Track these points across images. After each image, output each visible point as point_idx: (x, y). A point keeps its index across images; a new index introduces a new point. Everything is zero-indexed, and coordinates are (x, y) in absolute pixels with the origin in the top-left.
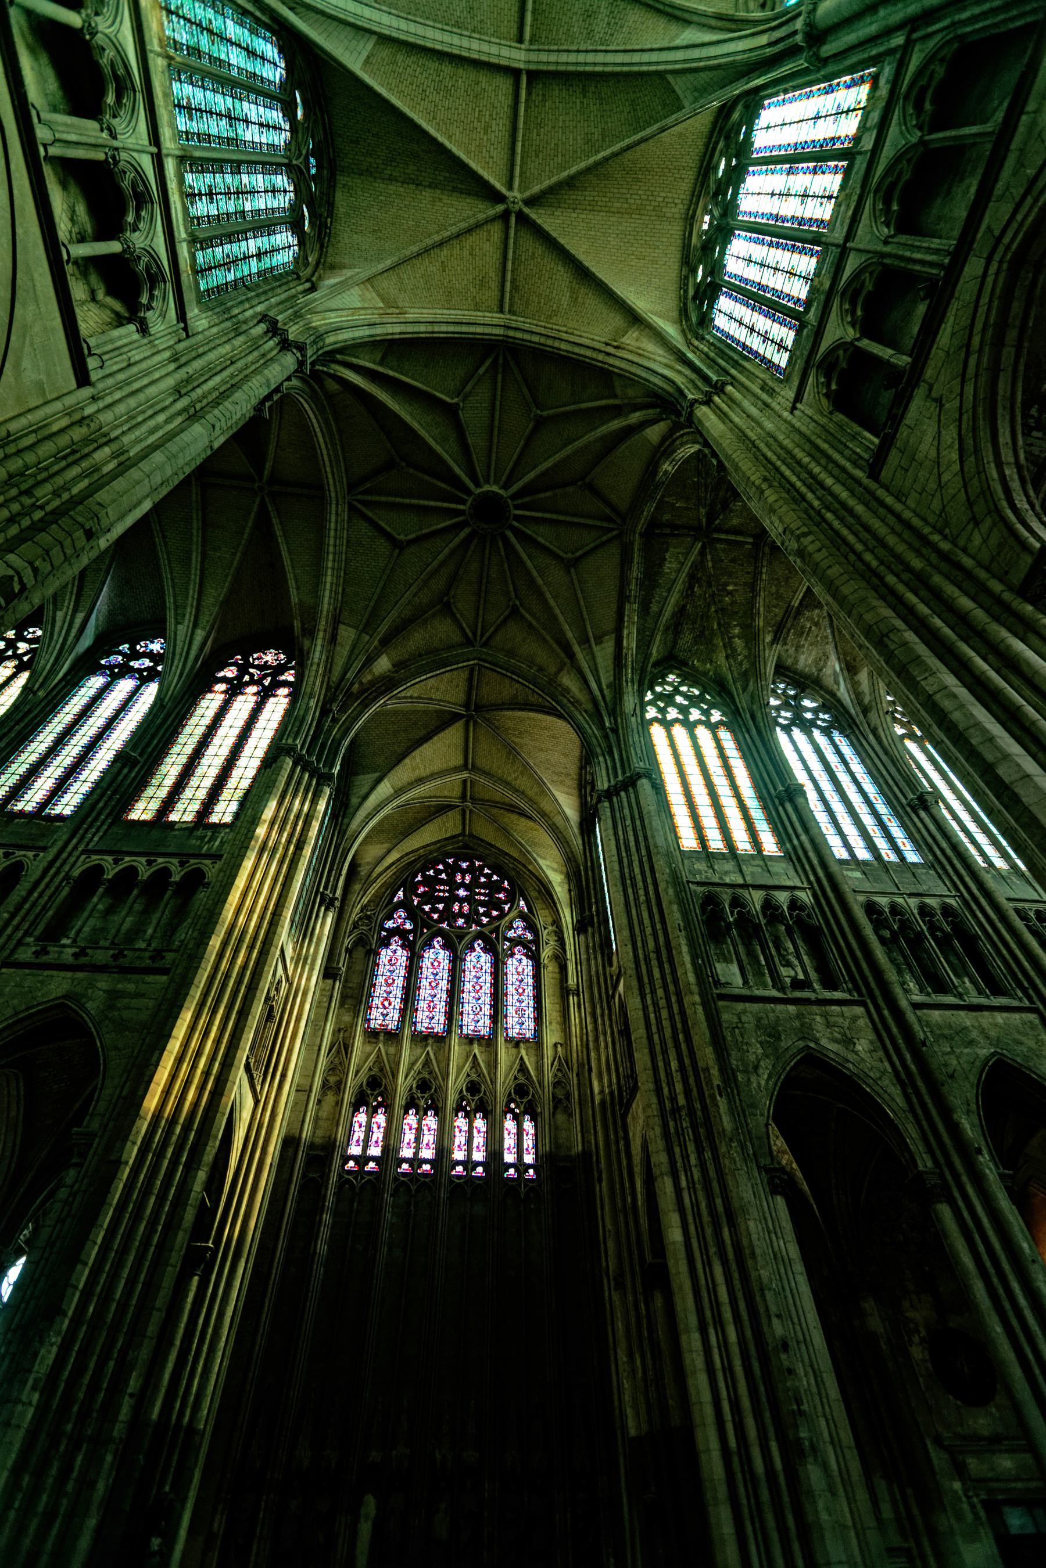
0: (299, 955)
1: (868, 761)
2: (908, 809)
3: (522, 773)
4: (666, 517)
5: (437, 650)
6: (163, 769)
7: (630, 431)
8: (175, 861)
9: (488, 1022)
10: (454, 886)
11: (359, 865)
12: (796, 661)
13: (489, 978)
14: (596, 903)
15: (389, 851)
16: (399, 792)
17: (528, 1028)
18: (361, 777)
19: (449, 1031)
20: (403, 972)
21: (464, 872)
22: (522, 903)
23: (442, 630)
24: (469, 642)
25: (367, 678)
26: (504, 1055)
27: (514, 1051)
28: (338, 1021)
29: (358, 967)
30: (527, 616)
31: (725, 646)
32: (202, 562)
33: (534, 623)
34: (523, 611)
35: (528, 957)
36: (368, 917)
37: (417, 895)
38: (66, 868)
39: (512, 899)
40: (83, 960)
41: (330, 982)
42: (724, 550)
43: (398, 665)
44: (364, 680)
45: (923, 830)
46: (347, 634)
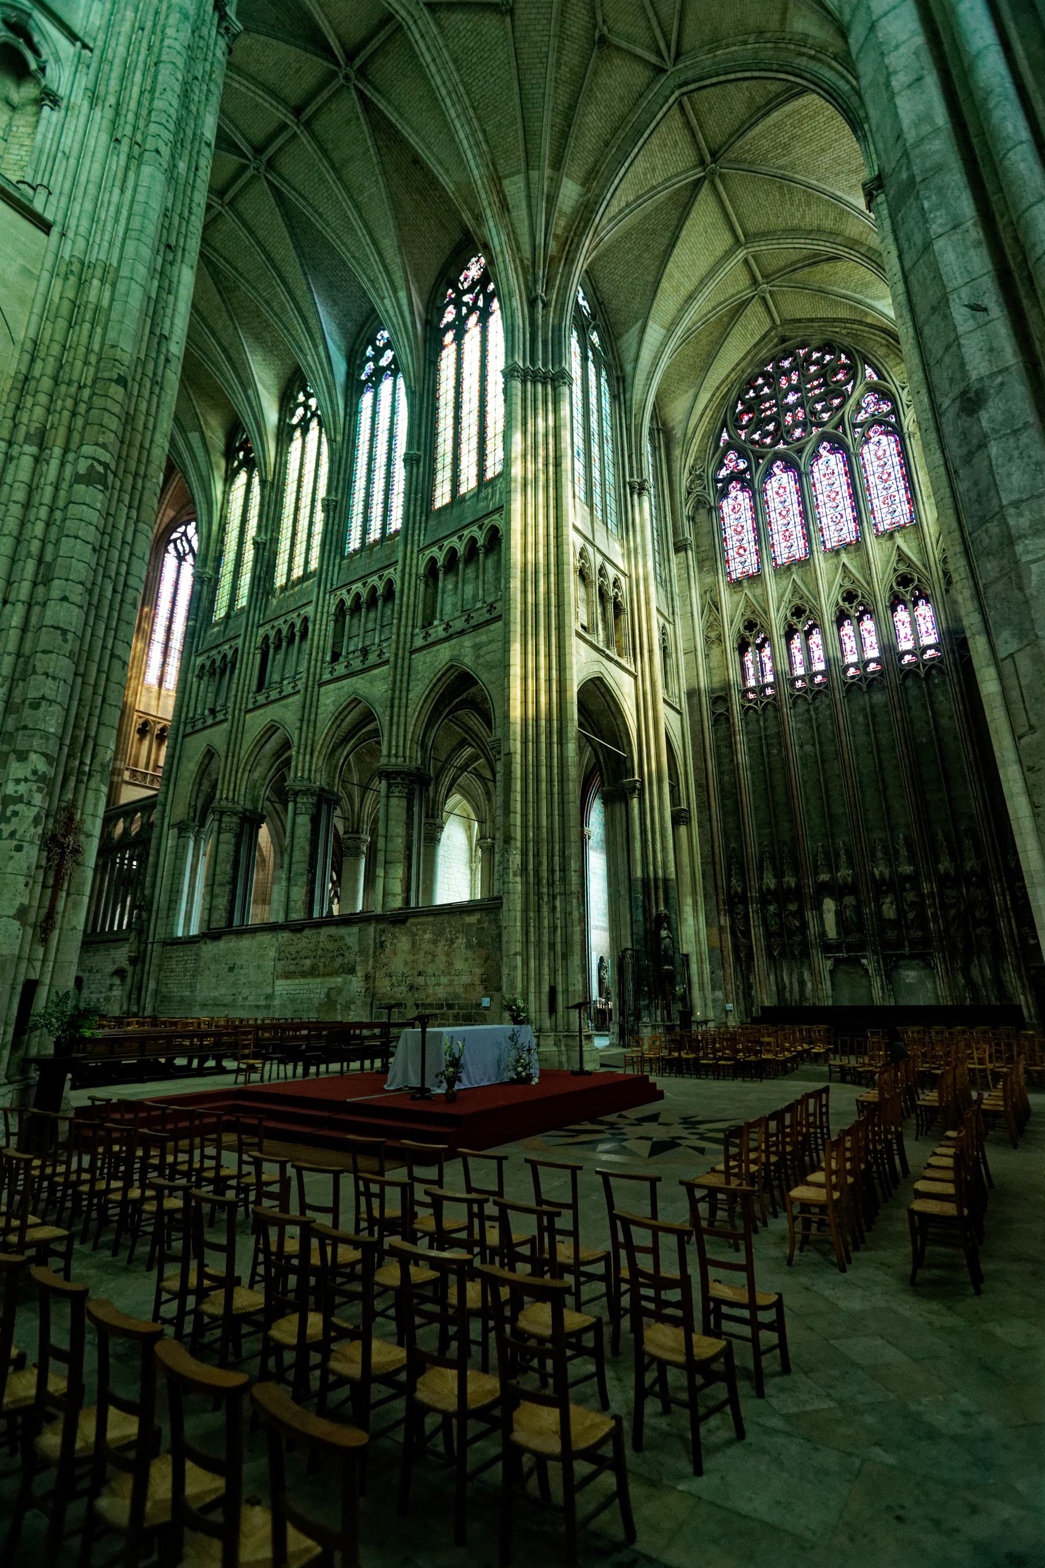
0: (628, 549)
5: (623, 119)
6: (440, 450)
8: (475, 528)
9: (852, 525)
10: (778, 395)
11: (673, 428)
13: (844, 479)
15: (696, 396)
17: (902, 513)
18: (625, 337)
19: (812, 552)
20: (749, 514)
21: (787, 373)
22: (869, 371)
25: (560, 224)
26: (877, 552)
27: (889, 544)
29: (706, 529)
35: (887, 434)
36: (700, 477)
37: (742, 428)
38: (414, 570)
39: (852, 372)
40: (451, 631)
41: (682, 554)
43: (586, 182)
44: (559, 231)
46: (514, 187)
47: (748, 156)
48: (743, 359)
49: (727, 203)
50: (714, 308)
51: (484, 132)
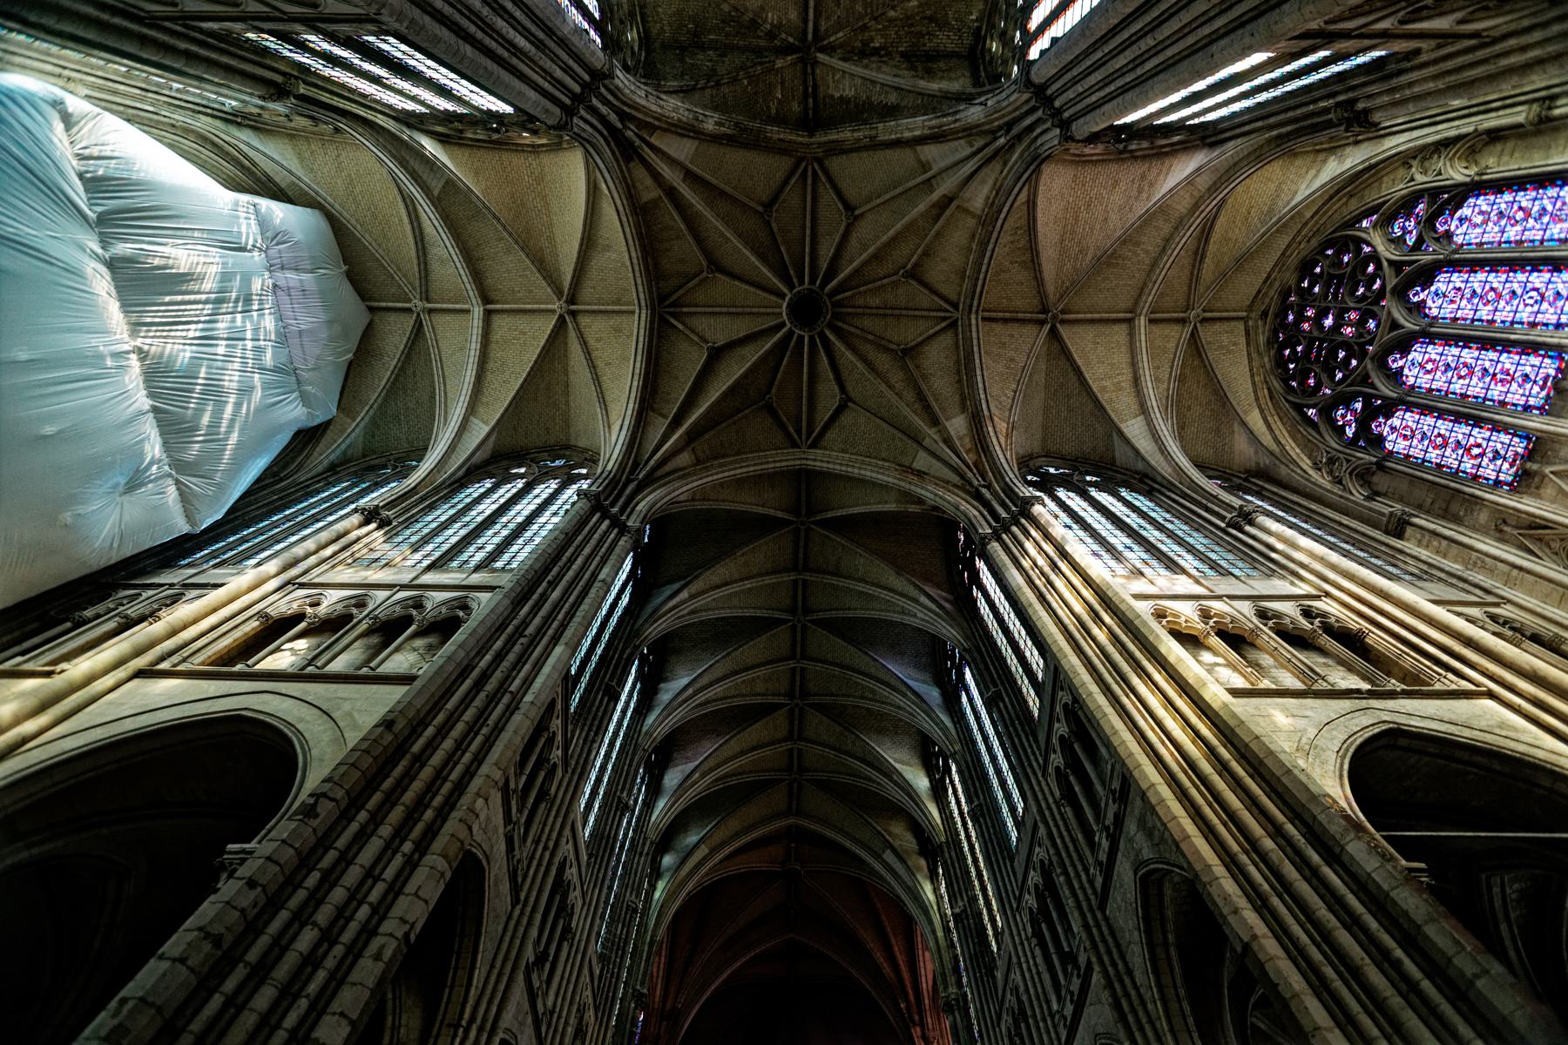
3: (1137, 244)
4: (796, 107)
7: (690, 176)
14: (1315, 101)
15: (1244, 424)
16: (1144, 410)
21: (1301, 318)
23: (937, 357)
24: (954, 325)
28: (1483, 530)
30: (913, 260)
32: (866, 582)
33: (919, 251)
34: (909, 266)
36: (1331, 461)
41: (1409, 531)
42: (828, 19)
44: (969, 446)
46: (922, 461)
47: (1068, 284)
48: (1250, 360)
49: (1089, 316)
50: (1172, 367)
51: (883, 460)
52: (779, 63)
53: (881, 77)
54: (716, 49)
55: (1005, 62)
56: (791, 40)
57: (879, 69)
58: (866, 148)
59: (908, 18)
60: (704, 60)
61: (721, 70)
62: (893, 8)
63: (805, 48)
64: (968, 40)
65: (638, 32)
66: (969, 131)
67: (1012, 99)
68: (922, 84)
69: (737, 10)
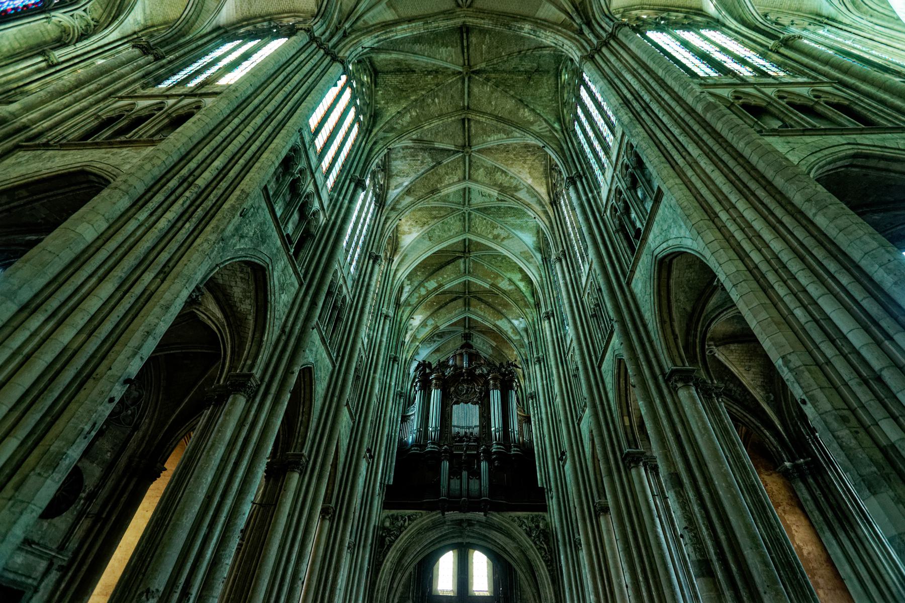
1: (373, 222)
2: (368, 254)
4: (474, 40)
12: (396, 159)
31: (405, 108)
42: (457, 88)
45: (365, 267)
52: (483, 65)
53: (425, 60)
54: (519, 71)
55: (358, 71)
56: (477, 78)
57: (427, 63)
58: (429, 16)
59: (415, 91)
60: (527, 65)
61: (517, 60)
62: (423, 95)
63: (470, 73)
64: (380, 80)
65: (561, 79)
66: (368, 30)
67: (348, 52)
68: (401, 57)
69: (506, 92)
